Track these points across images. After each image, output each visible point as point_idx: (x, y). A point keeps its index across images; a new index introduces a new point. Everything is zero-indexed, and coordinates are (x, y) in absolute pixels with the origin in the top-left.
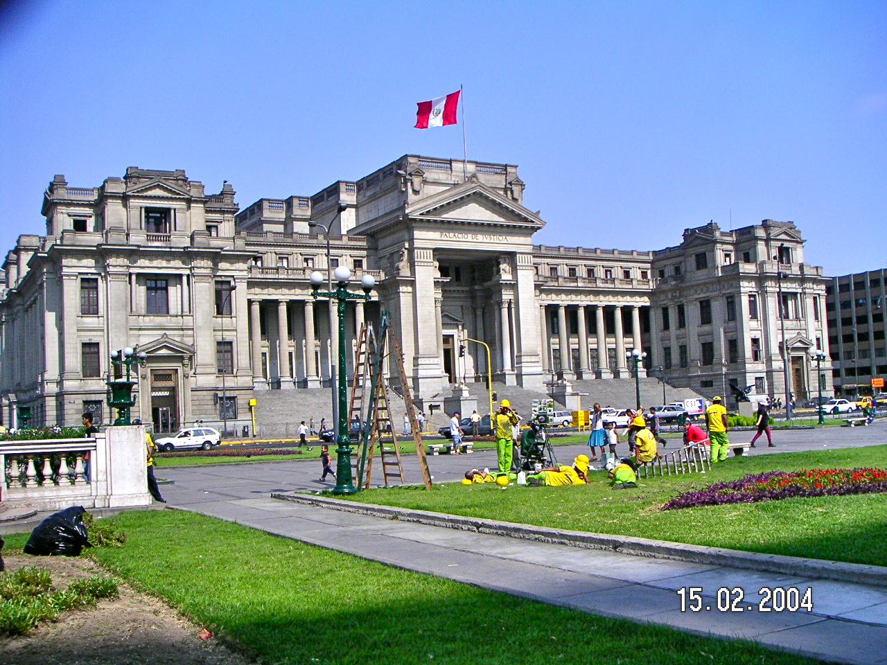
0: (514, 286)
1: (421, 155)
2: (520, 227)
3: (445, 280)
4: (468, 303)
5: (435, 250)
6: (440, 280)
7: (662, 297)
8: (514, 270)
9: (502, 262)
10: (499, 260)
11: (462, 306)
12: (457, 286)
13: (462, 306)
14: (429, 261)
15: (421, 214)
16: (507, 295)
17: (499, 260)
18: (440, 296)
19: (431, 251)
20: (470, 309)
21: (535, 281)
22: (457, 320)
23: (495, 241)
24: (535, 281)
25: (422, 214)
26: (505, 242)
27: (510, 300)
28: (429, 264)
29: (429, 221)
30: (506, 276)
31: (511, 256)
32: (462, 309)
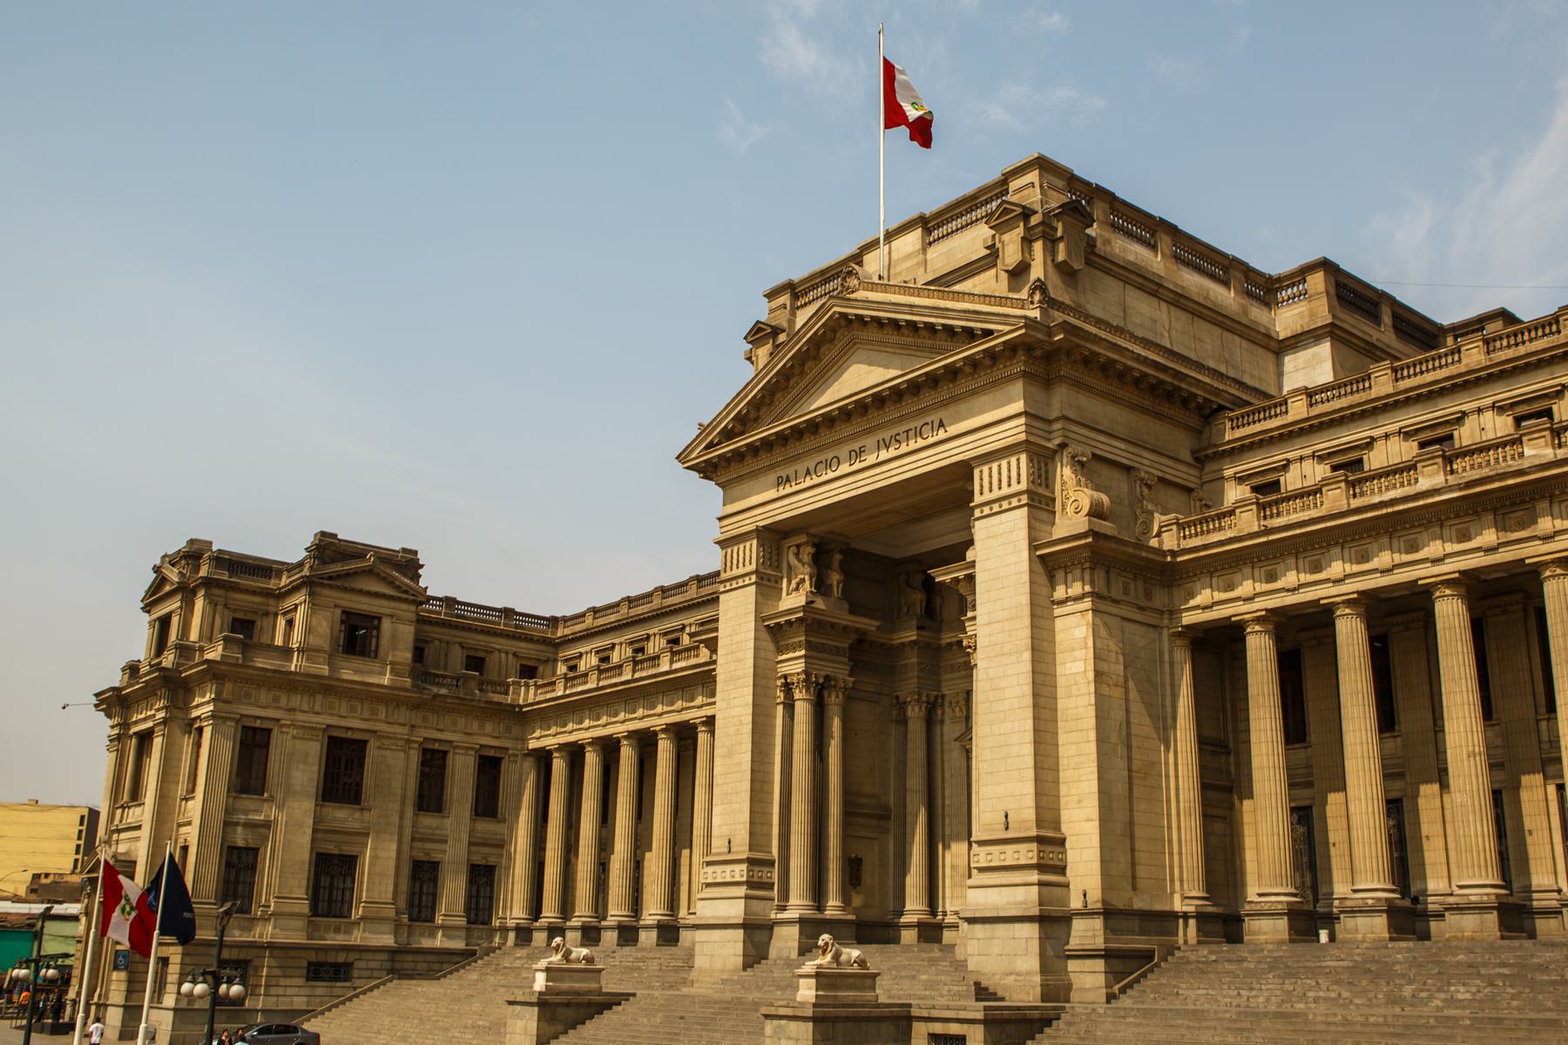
15: (707, 447)
18: (794, 664)
25: (710, 446)
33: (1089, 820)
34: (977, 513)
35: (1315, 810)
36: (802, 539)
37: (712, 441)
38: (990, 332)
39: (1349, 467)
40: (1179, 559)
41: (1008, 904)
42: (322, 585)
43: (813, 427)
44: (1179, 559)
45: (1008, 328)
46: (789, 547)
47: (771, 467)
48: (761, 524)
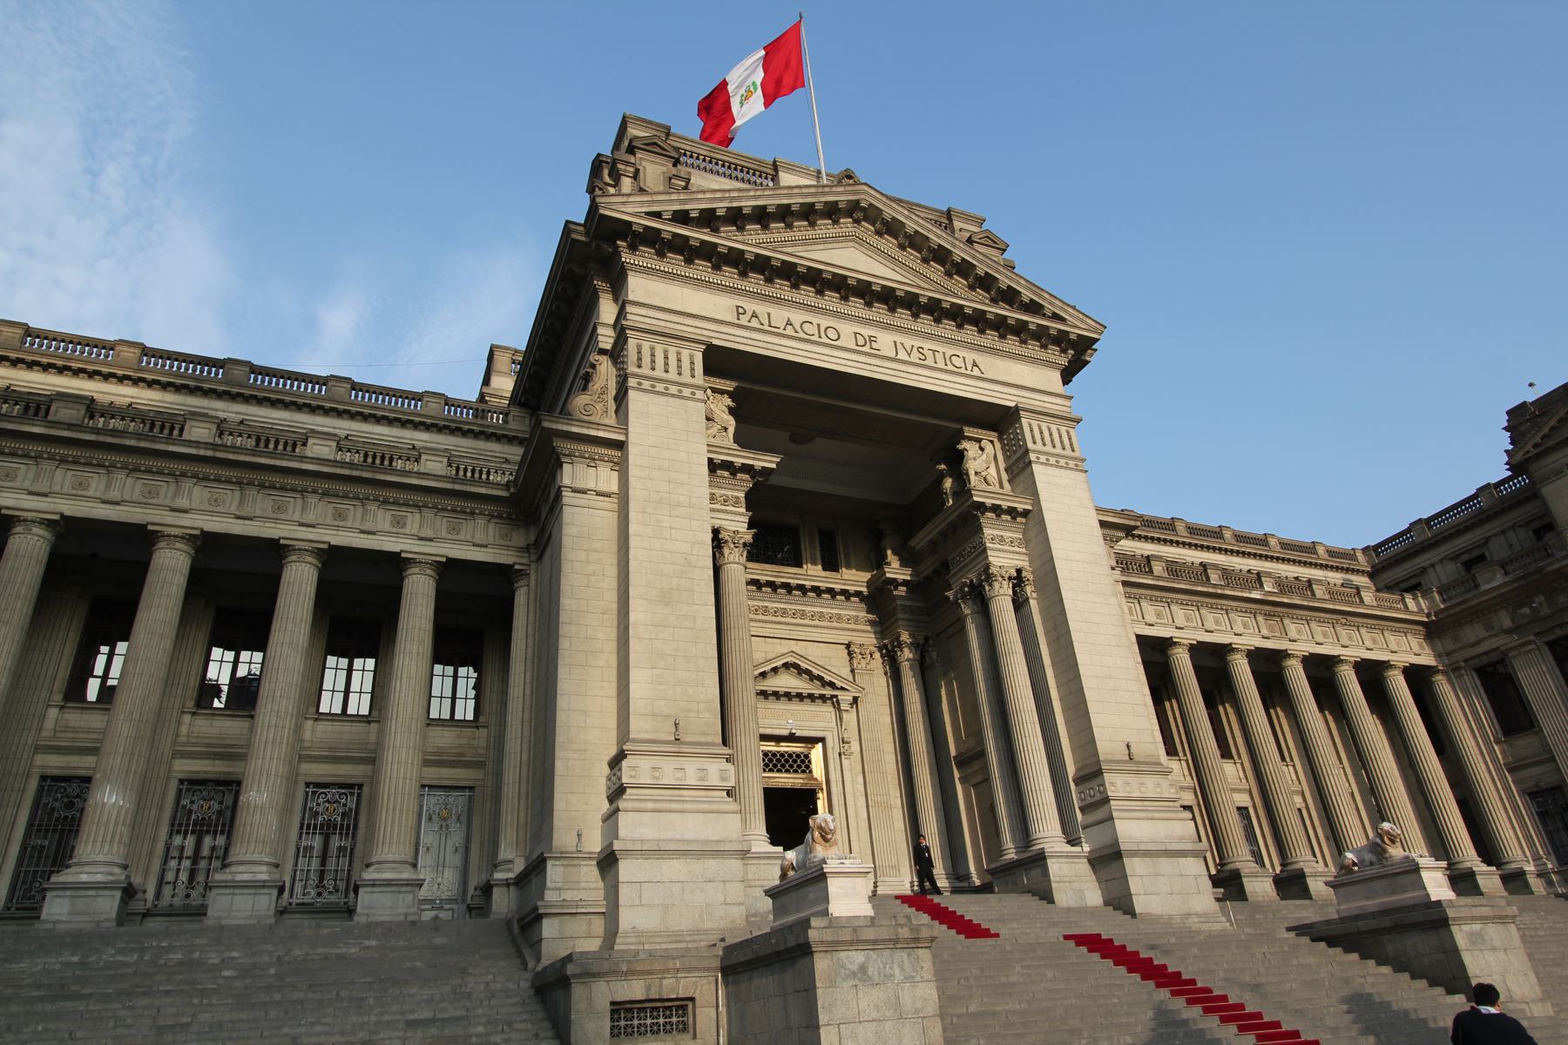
3: (758, 464)
4: (867, 639)
7: (1473, 632)
8: (1019, 466)
10: (960, 447)
11: (848, 646)
13: (848, 646)
15: (647, 213)
17: (960, 447)
18: (737, 523)
19: (699, 358)
20: (877, 655)
22: (832, 685)
23: (941, 365)
26: (976, 372)
27: (1019, 571)
31: (1000, 420)
32: (850, 654)
36: (729, 385)
47: (732, 290)
48: (715, 342)
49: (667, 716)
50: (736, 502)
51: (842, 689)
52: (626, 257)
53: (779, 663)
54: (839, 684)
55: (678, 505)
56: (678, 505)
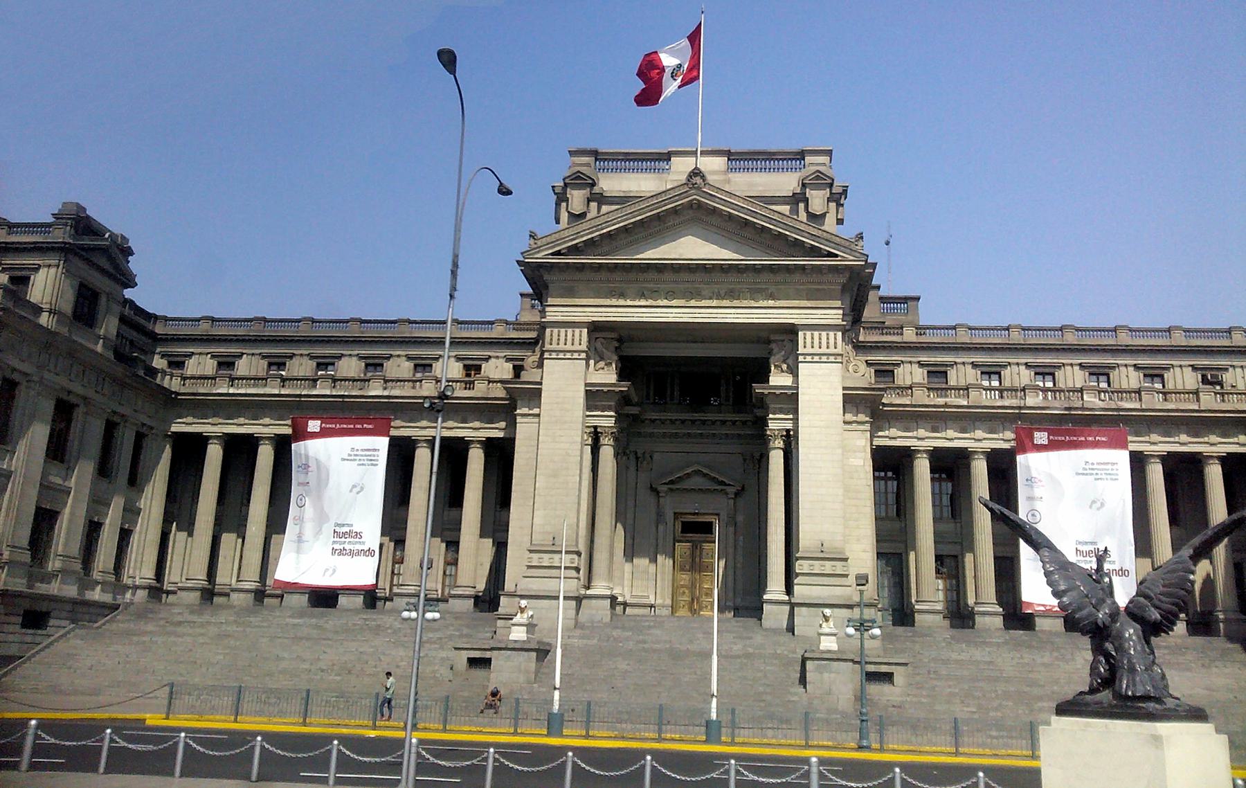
0: (790, 401)
1: (600, 151)
2: (803, 267)
5: (595, 328)
6: (617, 389)
9: (775, 351)
12: (739, 412)
14: (576, 347)
15: (552, 254)
16: (777, 423)
18: (607, 420)
21: (844, 388)
22: (722, 483)
24: (844, 388)
25: (558, 253)
28: (576, 355)
29: (581, 268)
30: (779, 379)
31: (790, 332)
33: (864, 551)
34: (801, 358)
35: (960, 557)
37: (560, 251)
38: (837, 256)
39: (938, 374)
40: (885, 409)
41: (829, 596)
42: (76, 254)
43: (660, 268)
44: (885, 409)
45: (852, 258)
46: (597, 338)
49: (550, 533)
50: (609, 409)
51: (729, 485)
52: (546, 277)
53: (689, 470)
54: (727, 482)
55: (566, 422)
56: (566, 422)
